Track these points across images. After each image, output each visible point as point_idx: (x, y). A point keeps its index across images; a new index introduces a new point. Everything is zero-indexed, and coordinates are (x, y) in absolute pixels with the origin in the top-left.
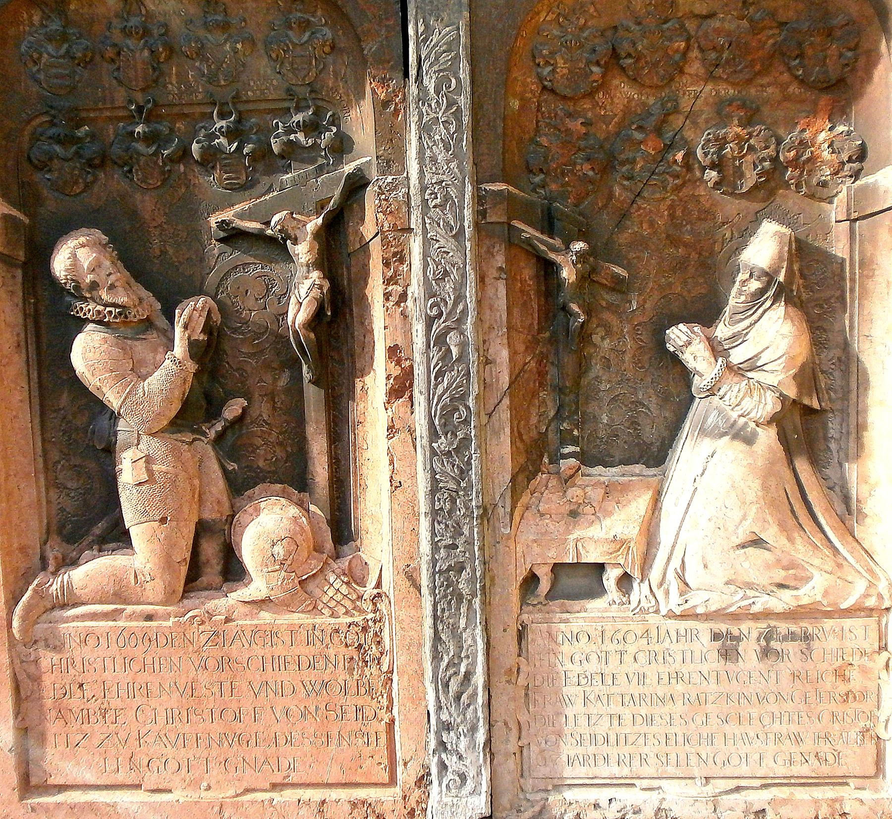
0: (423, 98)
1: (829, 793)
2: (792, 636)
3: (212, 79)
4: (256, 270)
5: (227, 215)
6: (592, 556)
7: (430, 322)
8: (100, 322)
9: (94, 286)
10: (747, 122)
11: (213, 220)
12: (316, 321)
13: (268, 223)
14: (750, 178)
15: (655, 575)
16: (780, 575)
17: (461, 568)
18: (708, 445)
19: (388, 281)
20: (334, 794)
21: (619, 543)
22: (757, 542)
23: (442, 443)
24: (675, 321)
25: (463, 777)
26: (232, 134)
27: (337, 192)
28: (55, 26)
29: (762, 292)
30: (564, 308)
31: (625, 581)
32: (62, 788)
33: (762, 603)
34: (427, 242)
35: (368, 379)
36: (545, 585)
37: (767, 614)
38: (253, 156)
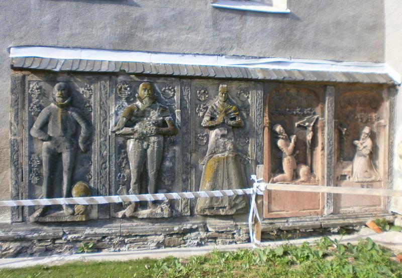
0: (328, 107)
1: (374, 208)
2: (371, 185)
3: (297, 103)
4: (302, 131)
5: (299, 123)
6: (346, 174)
7: (328, 139)
8: (282, 138)
9: (282, 133)
10: (365, 113)
11: (296, 124)
12: (312, 139)
13: (305, 124)
14: (365, 120)
15: (354, 176)
16: (369, 176)
17: (330, 175)
18: (360, 158)
19: (322, 133)
20: (311, 211)
21: (349, 172)
22: (366, 171)
23: (329, 157)
24: (355, 140)
25: (330, 207)
26: (300, 111)
27: (315, 120)
28: (277, 94)
29: (367, 137)
30: (343, 138)
31: (349, 177)
32: (273, 212)
33: (367, 180)
34: (328, 128)
35: (317, 148)
36: (339, 178)
37: (368, 182)
38: (302, 115)
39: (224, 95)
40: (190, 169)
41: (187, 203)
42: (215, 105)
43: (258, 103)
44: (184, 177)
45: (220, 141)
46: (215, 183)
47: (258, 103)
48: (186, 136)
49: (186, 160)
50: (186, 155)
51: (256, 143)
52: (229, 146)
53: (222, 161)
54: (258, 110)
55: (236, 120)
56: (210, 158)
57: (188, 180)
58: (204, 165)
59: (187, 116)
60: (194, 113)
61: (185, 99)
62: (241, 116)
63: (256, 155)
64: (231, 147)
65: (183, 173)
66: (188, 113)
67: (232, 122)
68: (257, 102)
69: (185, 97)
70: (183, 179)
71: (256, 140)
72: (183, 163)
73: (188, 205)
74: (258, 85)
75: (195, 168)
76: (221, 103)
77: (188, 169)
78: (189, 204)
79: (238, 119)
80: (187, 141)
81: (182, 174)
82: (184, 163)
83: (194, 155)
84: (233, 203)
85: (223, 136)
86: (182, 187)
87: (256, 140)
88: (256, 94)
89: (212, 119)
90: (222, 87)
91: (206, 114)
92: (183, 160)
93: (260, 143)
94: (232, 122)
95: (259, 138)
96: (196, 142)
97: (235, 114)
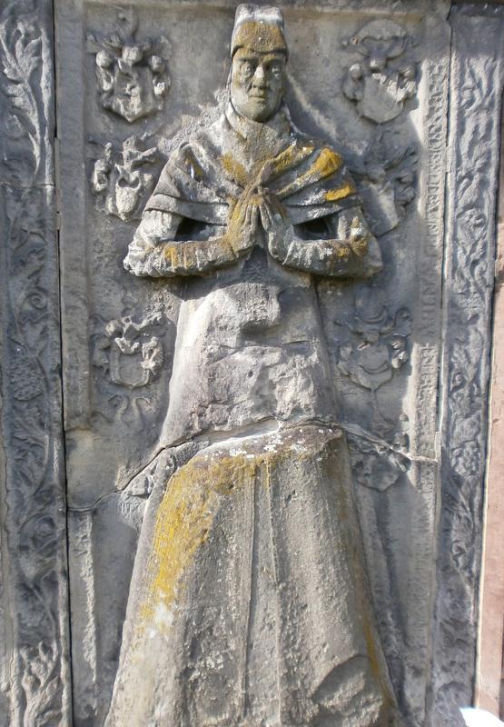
39: (259, 73)
40: (61, 526)
41: (55, 704)
42: (204, 140)
43: (468, 136)
44: (30, 571)
45: (232, 366)
46: (202, 609)
47: (468, 136)
48: (33, 334)
49: (39, 474)
50: (37, 445)
51: (451, 367)
52: (293, 391)
53: (249, 481)
54: (469, 176)
55: (334, 235)
56: (179, 461)
57: (53, 584)
58: (146, 495)
59: (33, 209)
60: (81, 192)
61: (18, 101)
62: (368, 210)
63: (448, 436)
64: (305, 399)
65: (23, 548)
66: (37, 189)
67: (308, 250)
68: (461, 131)
69: (11, 90)
70: (21, 576)
71: (451, 350)
72: (20, 495)
73: (59, 717)
74: (476, 20)
75: (95, 513)
76: (243, 127)
77: (51, 522)
78: (64, 708)
79: (350, 231)
80: (37, 365)
81: (15, 555)
82: (27, 491)
83: (85, 443)
84: (312, 710)
85: (254, 333)
86: (22, 626)
87: (451, 350)
88: (460, 86)
89: (189, 227)
90: (251, 23)
91: (153, 201)
92: (21, 476)
93: (471, 371)
94: (308, 250)
95: (466, 342)
96: (95, 368)
97: (331, 196)
